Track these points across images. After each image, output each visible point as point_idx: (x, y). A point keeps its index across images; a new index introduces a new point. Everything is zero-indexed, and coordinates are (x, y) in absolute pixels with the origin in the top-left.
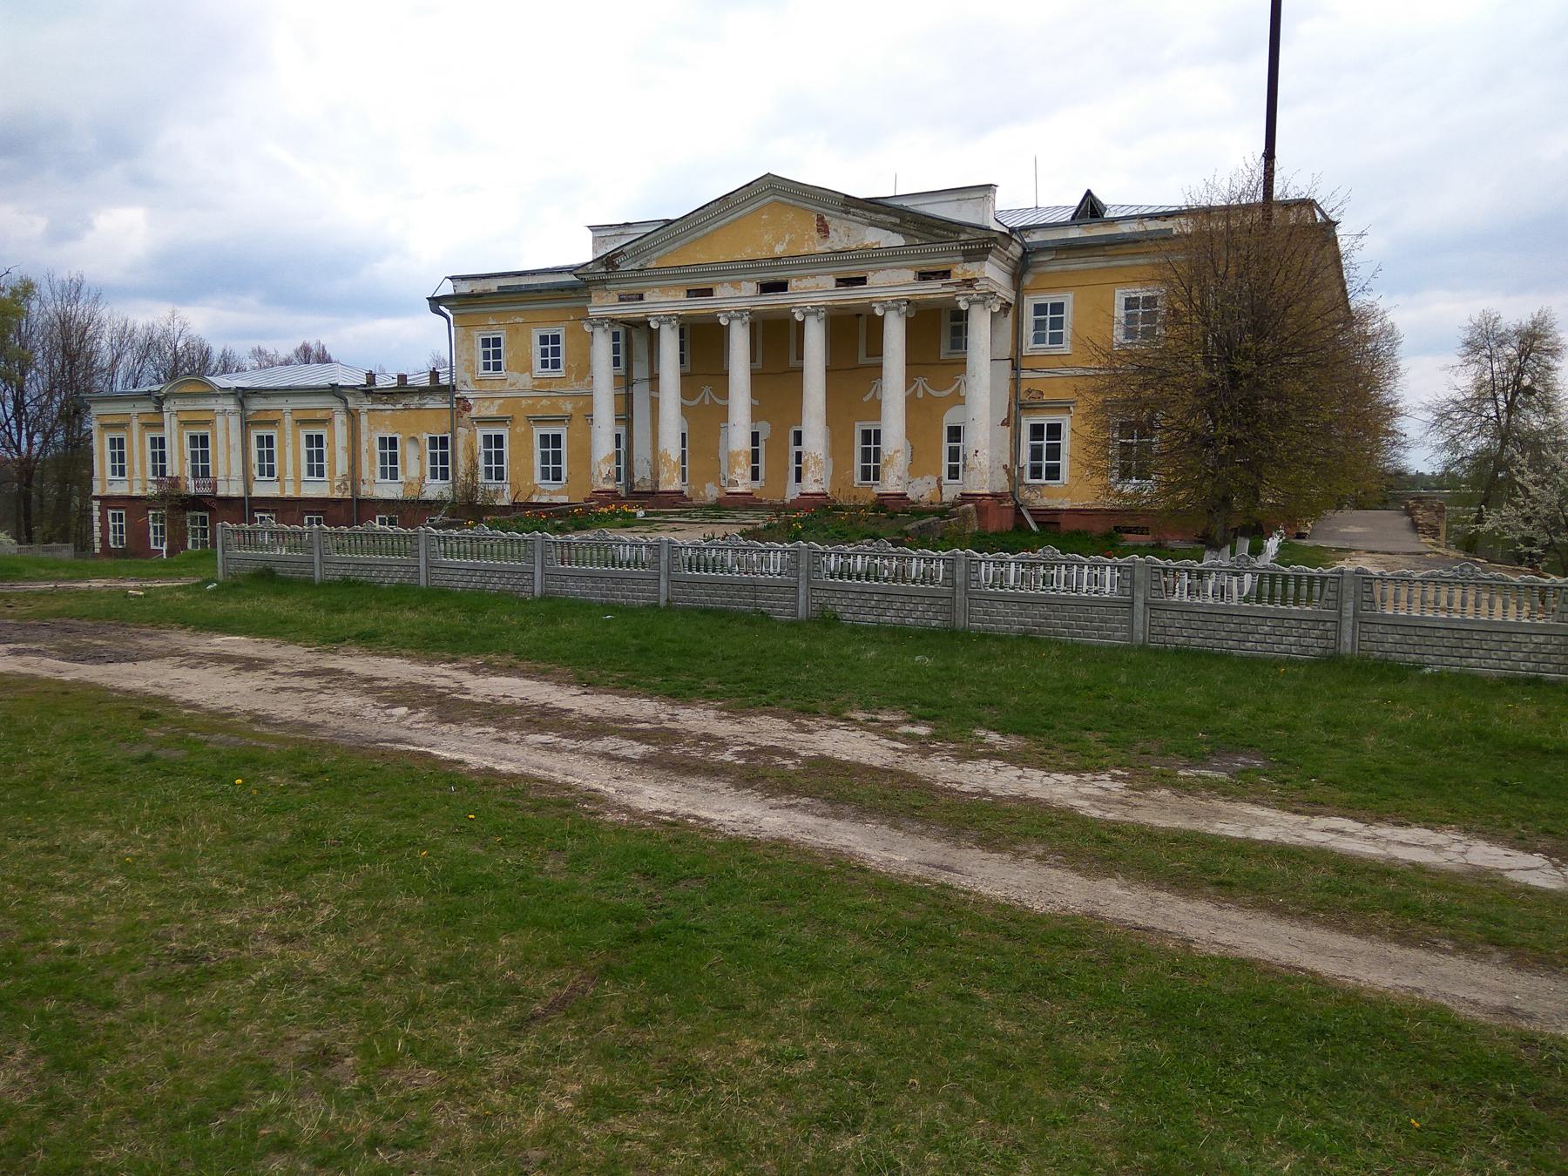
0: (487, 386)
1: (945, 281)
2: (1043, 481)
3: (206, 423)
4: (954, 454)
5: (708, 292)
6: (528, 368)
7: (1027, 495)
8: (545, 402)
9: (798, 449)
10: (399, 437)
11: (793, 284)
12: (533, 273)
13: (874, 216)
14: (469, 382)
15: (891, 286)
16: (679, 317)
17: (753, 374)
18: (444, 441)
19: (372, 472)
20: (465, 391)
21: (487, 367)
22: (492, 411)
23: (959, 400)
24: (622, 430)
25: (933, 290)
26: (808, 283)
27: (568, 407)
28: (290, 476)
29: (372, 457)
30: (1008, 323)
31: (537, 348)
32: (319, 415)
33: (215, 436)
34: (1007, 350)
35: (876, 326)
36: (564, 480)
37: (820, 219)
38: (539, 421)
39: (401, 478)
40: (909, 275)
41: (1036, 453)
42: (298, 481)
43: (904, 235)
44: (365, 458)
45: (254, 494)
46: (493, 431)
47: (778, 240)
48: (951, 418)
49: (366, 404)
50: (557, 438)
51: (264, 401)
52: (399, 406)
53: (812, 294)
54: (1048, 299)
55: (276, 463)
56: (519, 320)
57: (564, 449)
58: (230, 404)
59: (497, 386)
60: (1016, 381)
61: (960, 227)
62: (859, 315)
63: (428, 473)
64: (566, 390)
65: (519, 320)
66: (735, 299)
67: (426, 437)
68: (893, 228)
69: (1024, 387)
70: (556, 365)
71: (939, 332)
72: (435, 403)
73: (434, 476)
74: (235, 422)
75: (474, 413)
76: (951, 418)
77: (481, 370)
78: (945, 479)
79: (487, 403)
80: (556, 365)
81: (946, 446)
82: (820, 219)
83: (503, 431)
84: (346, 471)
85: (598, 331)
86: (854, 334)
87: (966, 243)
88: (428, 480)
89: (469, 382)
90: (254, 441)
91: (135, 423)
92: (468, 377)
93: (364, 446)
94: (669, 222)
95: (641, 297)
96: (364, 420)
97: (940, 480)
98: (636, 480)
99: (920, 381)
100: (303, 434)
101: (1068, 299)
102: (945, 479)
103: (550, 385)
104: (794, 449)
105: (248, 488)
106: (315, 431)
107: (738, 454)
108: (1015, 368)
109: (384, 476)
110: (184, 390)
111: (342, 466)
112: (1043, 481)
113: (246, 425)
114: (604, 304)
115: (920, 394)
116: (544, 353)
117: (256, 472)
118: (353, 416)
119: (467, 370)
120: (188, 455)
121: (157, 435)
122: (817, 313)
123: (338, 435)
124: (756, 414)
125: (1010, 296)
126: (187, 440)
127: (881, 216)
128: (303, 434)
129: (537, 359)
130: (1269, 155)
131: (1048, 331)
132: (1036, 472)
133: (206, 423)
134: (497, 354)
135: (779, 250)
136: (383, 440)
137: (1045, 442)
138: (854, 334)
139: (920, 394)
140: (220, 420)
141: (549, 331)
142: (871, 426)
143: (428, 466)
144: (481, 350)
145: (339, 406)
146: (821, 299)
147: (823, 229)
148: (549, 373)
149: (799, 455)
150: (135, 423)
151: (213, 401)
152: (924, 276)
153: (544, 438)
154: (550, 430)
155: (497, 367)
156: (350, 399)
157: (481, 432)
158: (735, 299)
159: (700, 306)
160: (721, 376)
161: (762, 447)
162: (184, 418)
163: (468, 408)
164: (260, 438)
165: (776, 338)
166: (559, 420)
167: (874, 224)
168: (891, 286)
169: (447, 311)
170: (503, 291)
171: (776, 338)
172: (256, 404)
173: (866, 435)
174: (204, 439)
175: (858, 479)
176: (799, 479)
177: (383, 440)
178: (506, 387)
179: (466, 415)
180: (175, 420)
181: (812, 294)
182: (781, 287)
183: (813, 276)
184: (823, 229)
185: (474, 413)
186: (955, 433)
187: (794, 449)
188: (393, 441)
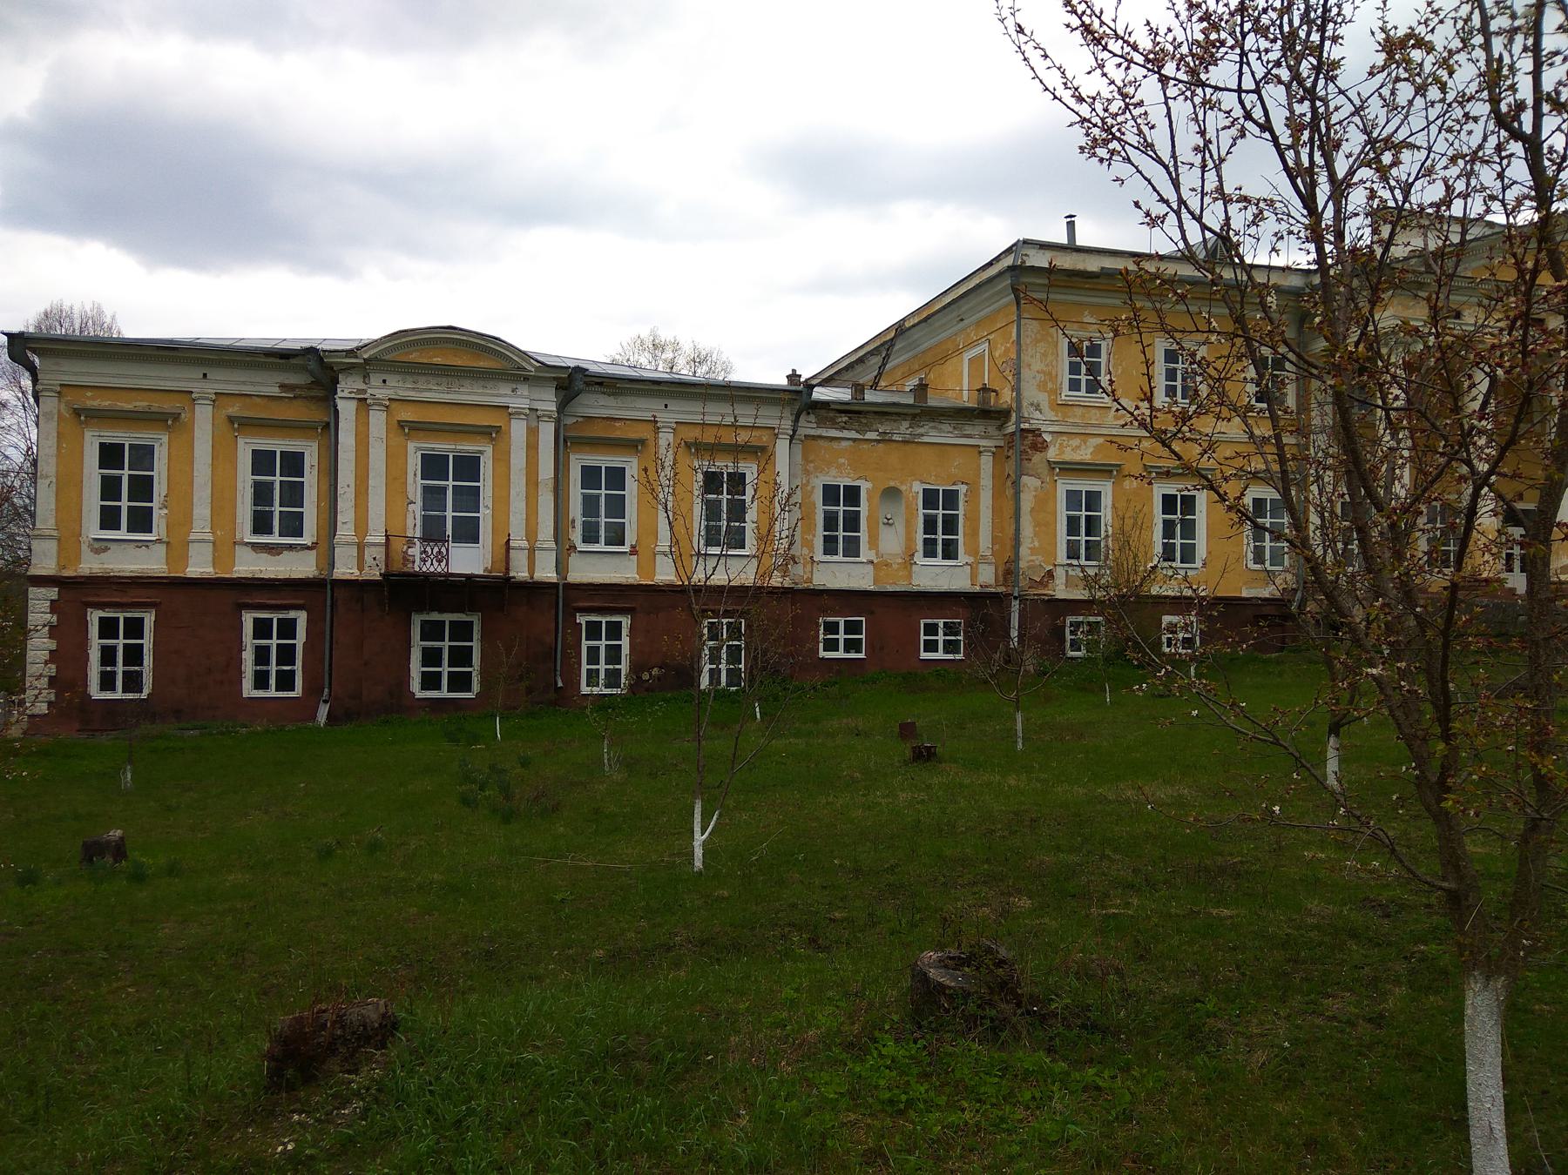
0: (1076, 416)
10: (865, 487)
14: (1045, 405)
21: (1075, 385)
22: (1084, 453)
33: (503, 459)
36: (1198, 564)
39: (866, 554)
45: (575, 576)
46: (1084, 485)
51: (611, 401)
58: (547, 401)
63: (920, 546)
67: (918, 488)
72: (980, 437)
73: (930, 552)
75: (1052, 454)
77: (1066, 391)
79: (1076, 442)
83: (1106, 489)
88: (919, 558)
89: (1045, 405)
90: (575, 475)
91: (203, 421)
92: (1043, 398)
105: (561, 566)
113: (565, 442)
117: (576, 536)
119: (1042, 386)
126: (414, 463)
136: (830, 494)
140: (518, 430)
143: (920, 536)
144: (1065, 360)
150: (203, 421)
151: (505, 389)
157: (1063, 486)
162: (408, 414)
170: (1105, 274)
172: (596, 405)
174: (469, 467)
179: (1037, 457)
180: (378, 420)
185: (1052, 454)
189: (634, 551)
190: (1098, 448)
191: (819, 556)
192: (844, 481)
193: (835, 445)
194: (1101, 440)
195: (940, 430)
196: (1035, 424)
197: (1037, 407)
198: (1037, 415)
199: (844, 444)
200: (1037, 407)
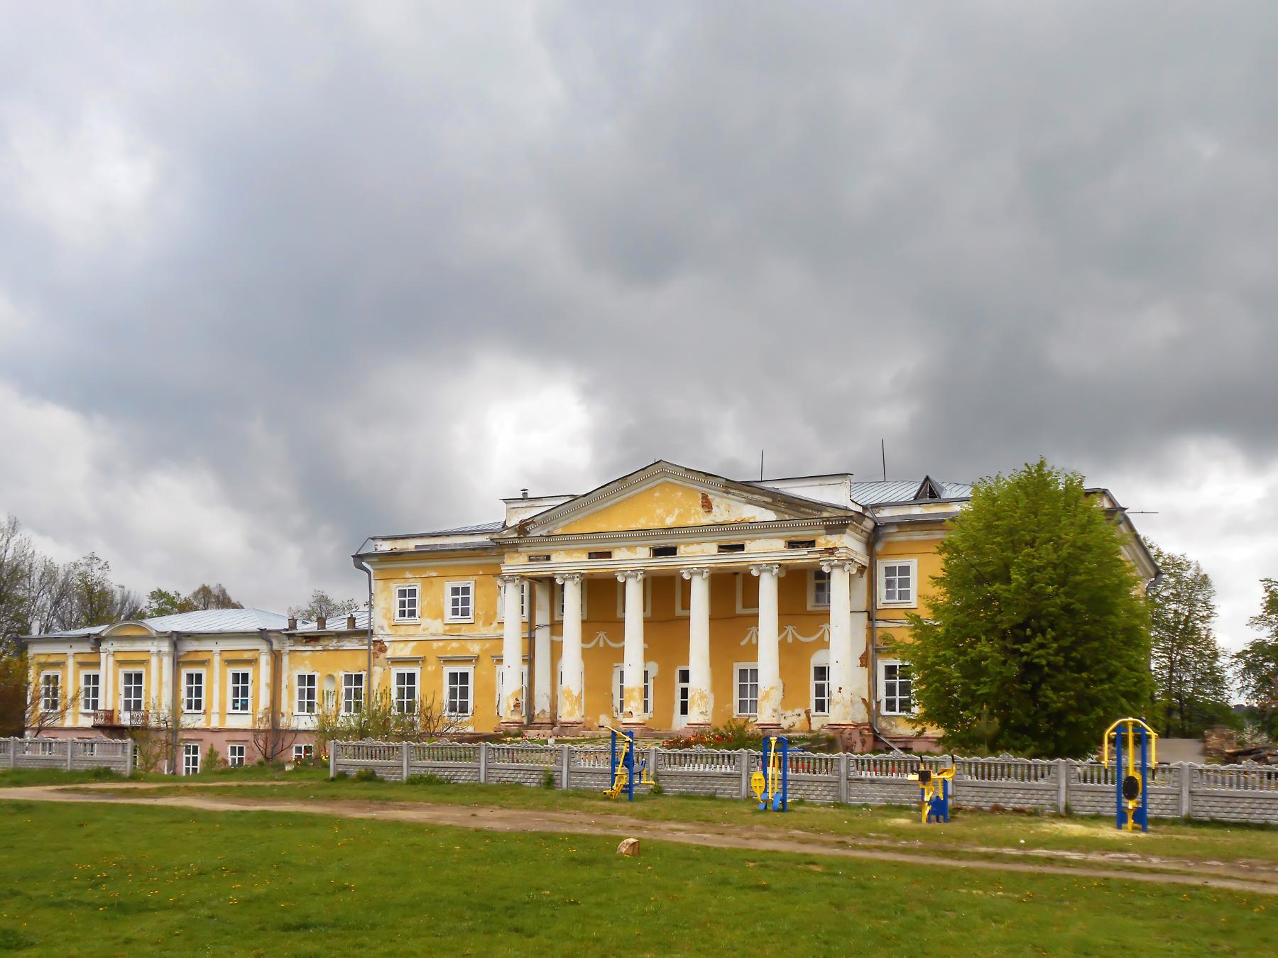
0: (402, 631)
1: (810, 549)
2: (897, 713)
3: (141, 663)
4: (820, 690)
5: (608, 555)
6: (440, 615)
7: (884, 724)
8: (455, 644)
9: (684, 685)
10: (317, 675)
11: (682, 550)
12: (448, 535)
13: (750, 496)
14: (386, 627)
15: (765, 552)
16: (582, 575)
17: (647, 622)
18: (359, 679)
19: (291, 706)
20: (380, 635)
21: (402, 614)
22: (405, 651)
23: (825, 645)
24: (525, 669)
25: (801, 556)
26: (694, 549)
27: (475, 649)
28: (216, 708)
30: (863, 581)
31: (449, 598)
32: (246, 656)
33: (149, 673)
34: (863, 606)
35: (750, 584)
36: (470, 713)
37: (705, 497)
38: (448, 661)
40: (781, 544)
41: (890, 690)
42: (223, 714)
43: (776, 511)
44: (285, 693)
46: (406, 670)
47: (669, 513)
48: (817, 660)
49: (288, 646)
50: (464, 676)
52: (319, 648)
53: (697, 557)
54: (897, 563)
55: (203, 698)
57: (470, 685)
58: (165, 646)
59: (412, 630)
60: (871, 630)
61: (821, 507)
62: (736, 574)
64: (475, 634)
66: (631, 560)
67: (342, 674)
69: (879, 633)
70: (465, 613)
71: (804, 589)
73: (348, 709)
74: (167, 662)
75: (389, 654)
76: (817, 660)
77: (397, 617)
78: (813, 712)
79: (402, 645)
80: (465, 613)
81: (813, 683)
82: (705, 497)
83: (416, 670)
84: (268, 705)
85: (509, 586)
86: (733, 590)
87: (828, 519)
89: (386, 627)
91: (71, 663)
92: (385, 623)
93: (285, 682)
94: (575, 498)
95: (548, 558)
96: (286, 659)
97: (807, 712)
98: (536, 712)
99: (790, 629)
100: (231, 671)
101: (913, 563)
102: (813, 712)
103: (459, 630)
104: (679, 686)
107: (633, 690)
108: (870, 619)
109: (301, 708)
110: (128, 633)
111: (264, 700)
112: (897, 713)
113: (177, 664)
114: (515, 563)
115: (790, 640)
116: (455, 602)
117: (184, 706)
118: (276, 657)
120: (122, 691)
121: (91, 672)
122: (702, 574)
123: (261, 675)
124: (648, 656)
125: (863, 559)
126: (122, 678)
127: (756, 497)
128: (231, 671)
129: (448, 608)
131: (897, 589)
132: (890, 705)
133: (141, 663)
134: (413, 603)
135: (670, 521)
136: (301, 678)
137: (898, 680)
138: (733, 590)
139: (790, 640)
140: (154, 660)
141: (459, 584)
142: (748, 666)
144: (397, 600)
145: (263, 646)
146: (705, 562)
147: (707, 505)
148: (459, 619)
149: (685, 692)
150: (71, 663)
151: (149, 643)
152: (792, 545)
153: (453, 676)
154: (459, 669)
155: (412, 613)
156: (275, 642)
157: (396, 670)
158: (631, 560)
159: (600, 566)
160: (616, 626)
161: (651, 683)
162: (120, 657)
163: (383, 650)
164: (190, 676)
165: (666, 593)
166: (467, 661)
167: (750, 502)
168: (765, 552)
169: (368, 566)
171: (666, 593)
173: (743, 673)
174: (139, 677)
175: (736, 712)
176: (684, 710)
177: (301, 678)
179: (382, 656)
180: (111, 660)
181: (697, 557)
182: (671, 551)
183: (699, 543)
184: (707, 505)
185: (389, 654)
186: (822, 672)
187: (679, 686)
188: (311, 679)
189: (205, 713)
190: (414, 648)
191: (296, 712)
192: (307, 673)
196: (380, 638)
197: (382, 628)
200: (382, 628)
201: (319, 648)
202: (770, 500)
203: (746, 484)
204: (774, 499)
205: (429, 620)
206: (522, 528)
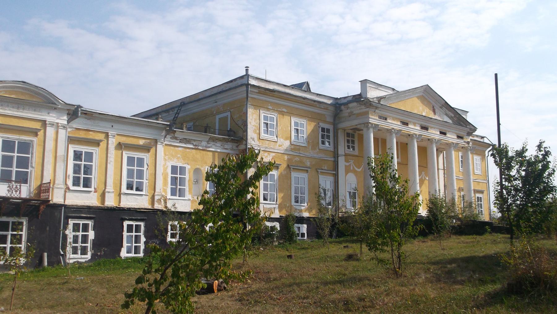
3: (35, 133)
10: (188, 167)
14: (256, 139)
29: (165, 179)
56: (284, 110)
59: (272, 145)
65: (284, 110)
68: (451, 118)
92: (255, 136)
95: (386, 119)
99: (423, 173)
106: (84, 149)
130: (499, 124)
133: (35, 133)
140: (50, 131)
167: (446, 115)
174: (25, 147)
178: (277, 147)
192: (179, 164)
193: (177, 148)
194: (274, 154)
195: (216, 146)
197: (253, 139)
198: (253, 142)
199: (180, 149)
200: (253, 139)
201: (192, 146)
202: (453, 115)
203: (453, 108)
204: (455, 116)
205: (282, 140)
206: (380, 99)
